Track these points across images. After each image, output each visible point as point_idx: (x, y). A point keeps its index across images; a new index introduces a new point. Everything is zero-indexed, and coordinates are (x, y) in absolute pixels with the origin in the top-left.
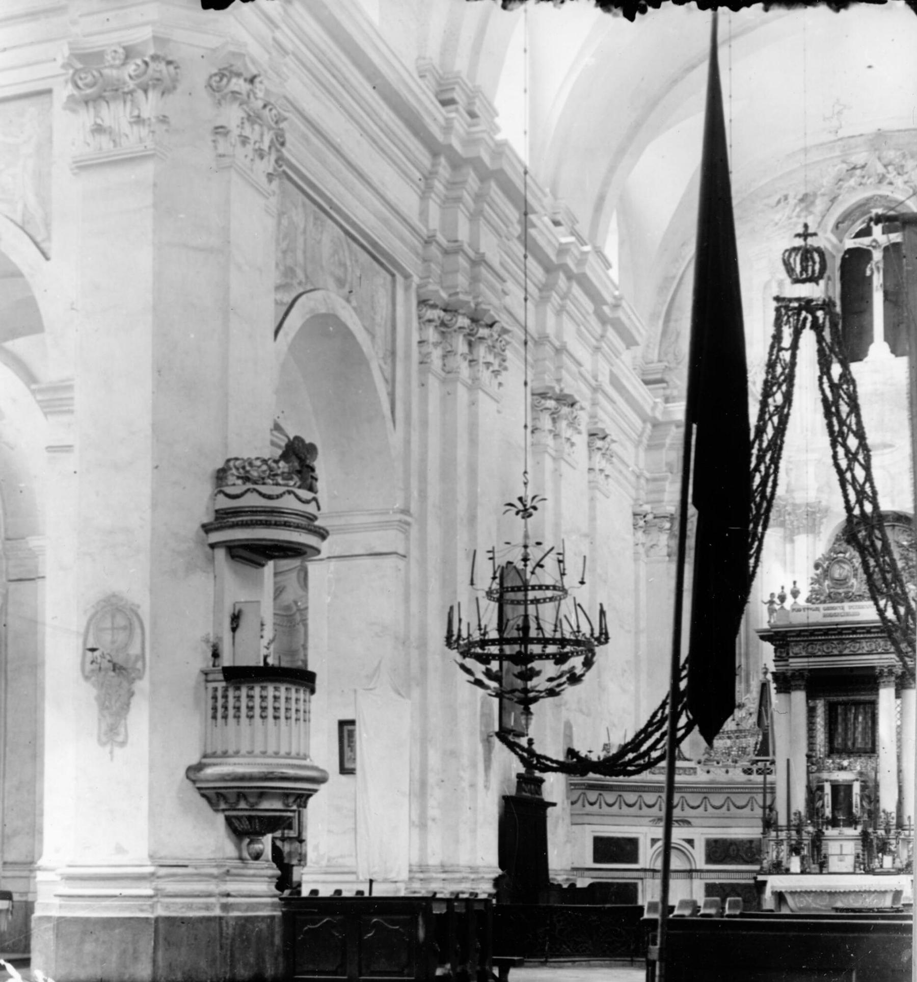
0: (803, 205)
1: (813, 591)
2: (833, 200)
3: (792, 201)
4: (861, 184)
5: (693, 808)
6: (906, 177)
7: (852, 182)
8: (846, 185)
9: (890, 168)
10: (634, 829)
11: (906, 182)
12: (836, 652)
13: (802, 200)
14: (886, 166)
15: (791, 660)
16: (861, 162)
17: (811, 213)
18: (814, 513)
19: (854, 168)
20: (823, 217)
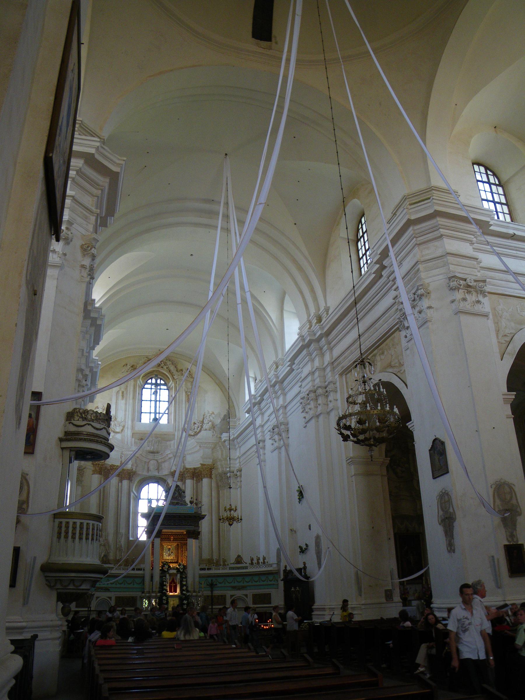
5: (128, 584)
6: (167, 366)
11: (167, 368)
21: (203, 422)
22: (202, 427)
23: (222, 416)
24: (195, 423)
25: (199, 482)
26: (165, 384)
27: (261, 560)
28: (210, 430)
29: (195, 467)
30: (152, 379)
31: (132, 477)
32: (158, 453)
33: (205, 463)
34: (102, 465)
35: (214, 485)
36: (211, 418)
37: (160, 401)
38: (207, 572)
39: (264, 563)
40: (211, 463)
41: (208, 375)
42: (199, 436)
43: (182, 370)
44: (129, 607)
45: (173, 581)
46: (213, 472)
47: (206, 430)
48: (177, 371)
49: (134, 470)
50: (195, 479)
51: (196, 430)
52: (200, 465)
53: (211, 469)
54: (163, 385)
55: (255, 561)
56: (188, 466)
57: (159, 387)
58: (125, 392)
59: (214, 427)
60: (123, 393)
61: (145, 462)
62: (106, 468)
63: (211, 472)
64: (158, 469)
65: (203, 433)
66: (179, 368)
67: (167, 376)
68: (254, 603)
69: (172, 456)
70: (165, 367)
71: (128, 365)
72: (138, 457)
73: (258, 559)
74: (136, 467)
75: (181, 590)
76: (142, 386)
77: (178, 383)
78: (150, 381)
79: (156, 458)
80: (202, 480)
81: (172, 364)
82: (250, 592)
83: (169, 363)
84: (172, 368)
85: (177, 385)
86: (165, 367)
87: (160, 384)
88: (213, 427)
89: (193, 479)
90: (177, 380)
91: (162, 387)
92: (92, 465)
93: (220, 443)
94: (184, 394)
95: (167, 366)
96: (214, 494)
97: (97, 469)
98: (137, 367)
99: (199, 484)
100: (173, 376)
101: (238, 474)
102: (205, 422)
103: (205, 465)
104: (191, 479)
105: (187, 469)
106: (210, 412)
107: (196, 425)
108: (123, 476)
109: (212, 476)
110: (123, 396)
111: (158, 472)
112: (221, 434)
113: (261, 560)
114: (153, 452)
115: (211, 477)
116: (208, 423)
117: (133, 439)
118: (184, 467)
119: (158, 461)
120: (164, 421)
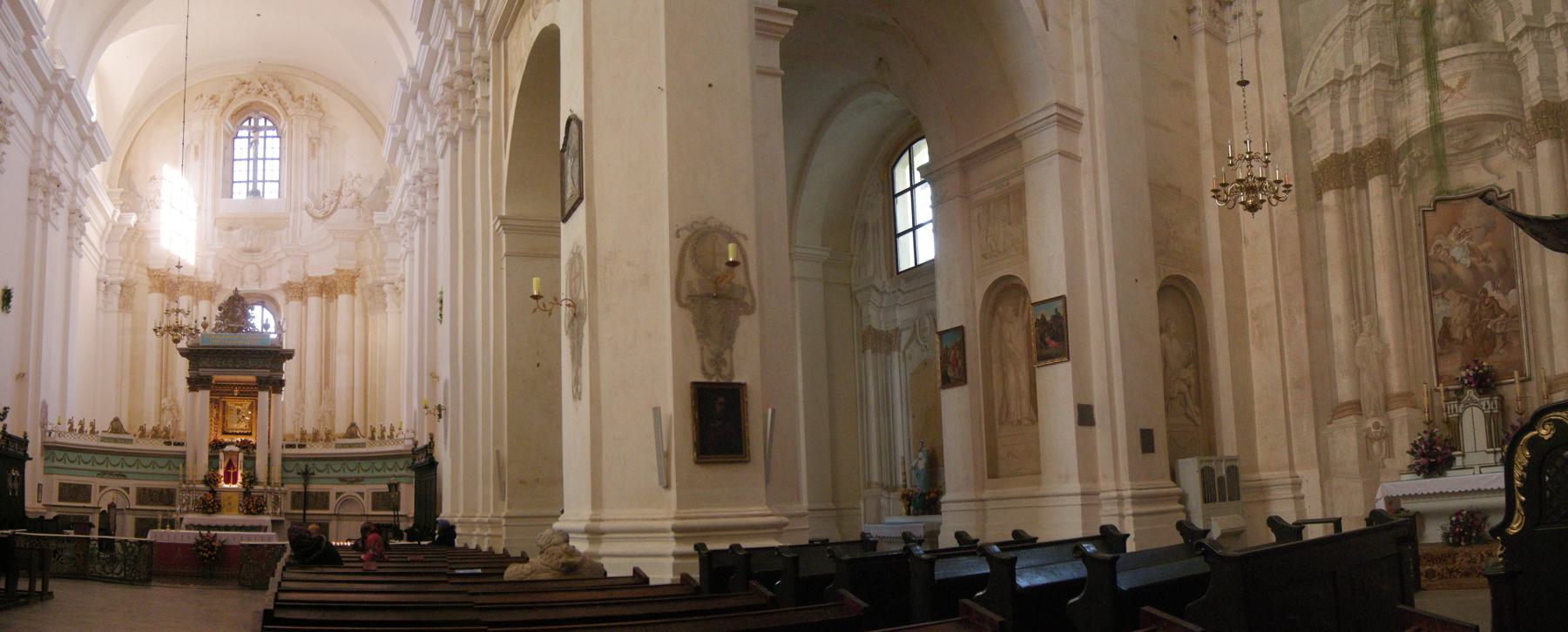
0: (212, 102)
1: (216, 324)
2: (230, 101)
3: (205, 98)
4: (247, 93)
7: (242, 91)
8: (238, 94)
9: (265, 86)
10: (90, 479)
12: (231, 366)
13: (212, 99)
14: (263, 85)
15: (200, 370)
16: (248, 81)
17: (216, 107)
18: (211, 288)
19: (244, 83)
20: (224, 110)
21: (339, 193)
22: (338, 202)
23: (376, 181)
24: (325, 196)
25: (332, 301)
26: (274, 127)
27: (387, 433)
28: (353, 208)
29: (325, 274)
30: (250, 119)
31: (216, 294)
32: (259, 251)
33: (342, 268)
34: (164, 277)
35: (358, 305)
36: (356, 186)
37: (264, 159)
38: (296, 451)
39: (391, 436)
40: (354, 268)
41: (352, 104)
42: (331, 220)
43: (302, 98)
44: (161, 505)
45: (230, 465)
46: (357, 284)
47: (346, 207)
48: (293, 99)
49: (218, 282)
50: (324, 295)
51: (326, 209)
52: (334, 272)
53: (353, 277)
54: (270, 128)
55: (377, 434)
56: (312, 274)
57: (262, 133)
58: (200, 147)
59: (360, 202)
60: (196, 148)
61: (237, 268)
62: (171, 282)
63: (354, 283)
64: (259, 280)
65: (340, 213)
66: (297, 94)
67: (276, 111)
68: (374, 508)
69: (284, 255)
70: (271, 94)
71: (204, 97)
72: (224, 260)
73: (383, 430)
74: (222, 276)
75: (243, 482)
76: (232, 133)
77: (294, 122)
78: (246, 124)
79: (256, 261)
80: (337, 297)
81: (285, 87)
82: (368, 488)
83: (277, 85)
84: (284, 95)
85: (293, 127)
86: (271, 94)
87: (266, 128)
88: (359, 201)
89: (321, 296)
90: (293, 117)
91: (269, 133)
92: (148, 278)
93: (371, 232)
94: (306, 142)
95: (275, 93)
96: (358, 321)
97: (157, 283)
98: (220, 98)
99: (331, 304)
100: (285, 110)
101: (401, 285)
102: (345, 192)
103: (342, 271)
104: (317, 296)
105: (310, 278)
106: (354, 175)
107: (326, 199)
108: (200, 294)
109: (356, 290)
110: (196, 154)
111: (260, 285)
112: (372, 215)
113: (387, 433)
114: (250, 251)
115: (352, 292)
116: (350, 195)
117: (216, 229)
118: (305, 275)
119: (258, 267)
120: (271, 192)
